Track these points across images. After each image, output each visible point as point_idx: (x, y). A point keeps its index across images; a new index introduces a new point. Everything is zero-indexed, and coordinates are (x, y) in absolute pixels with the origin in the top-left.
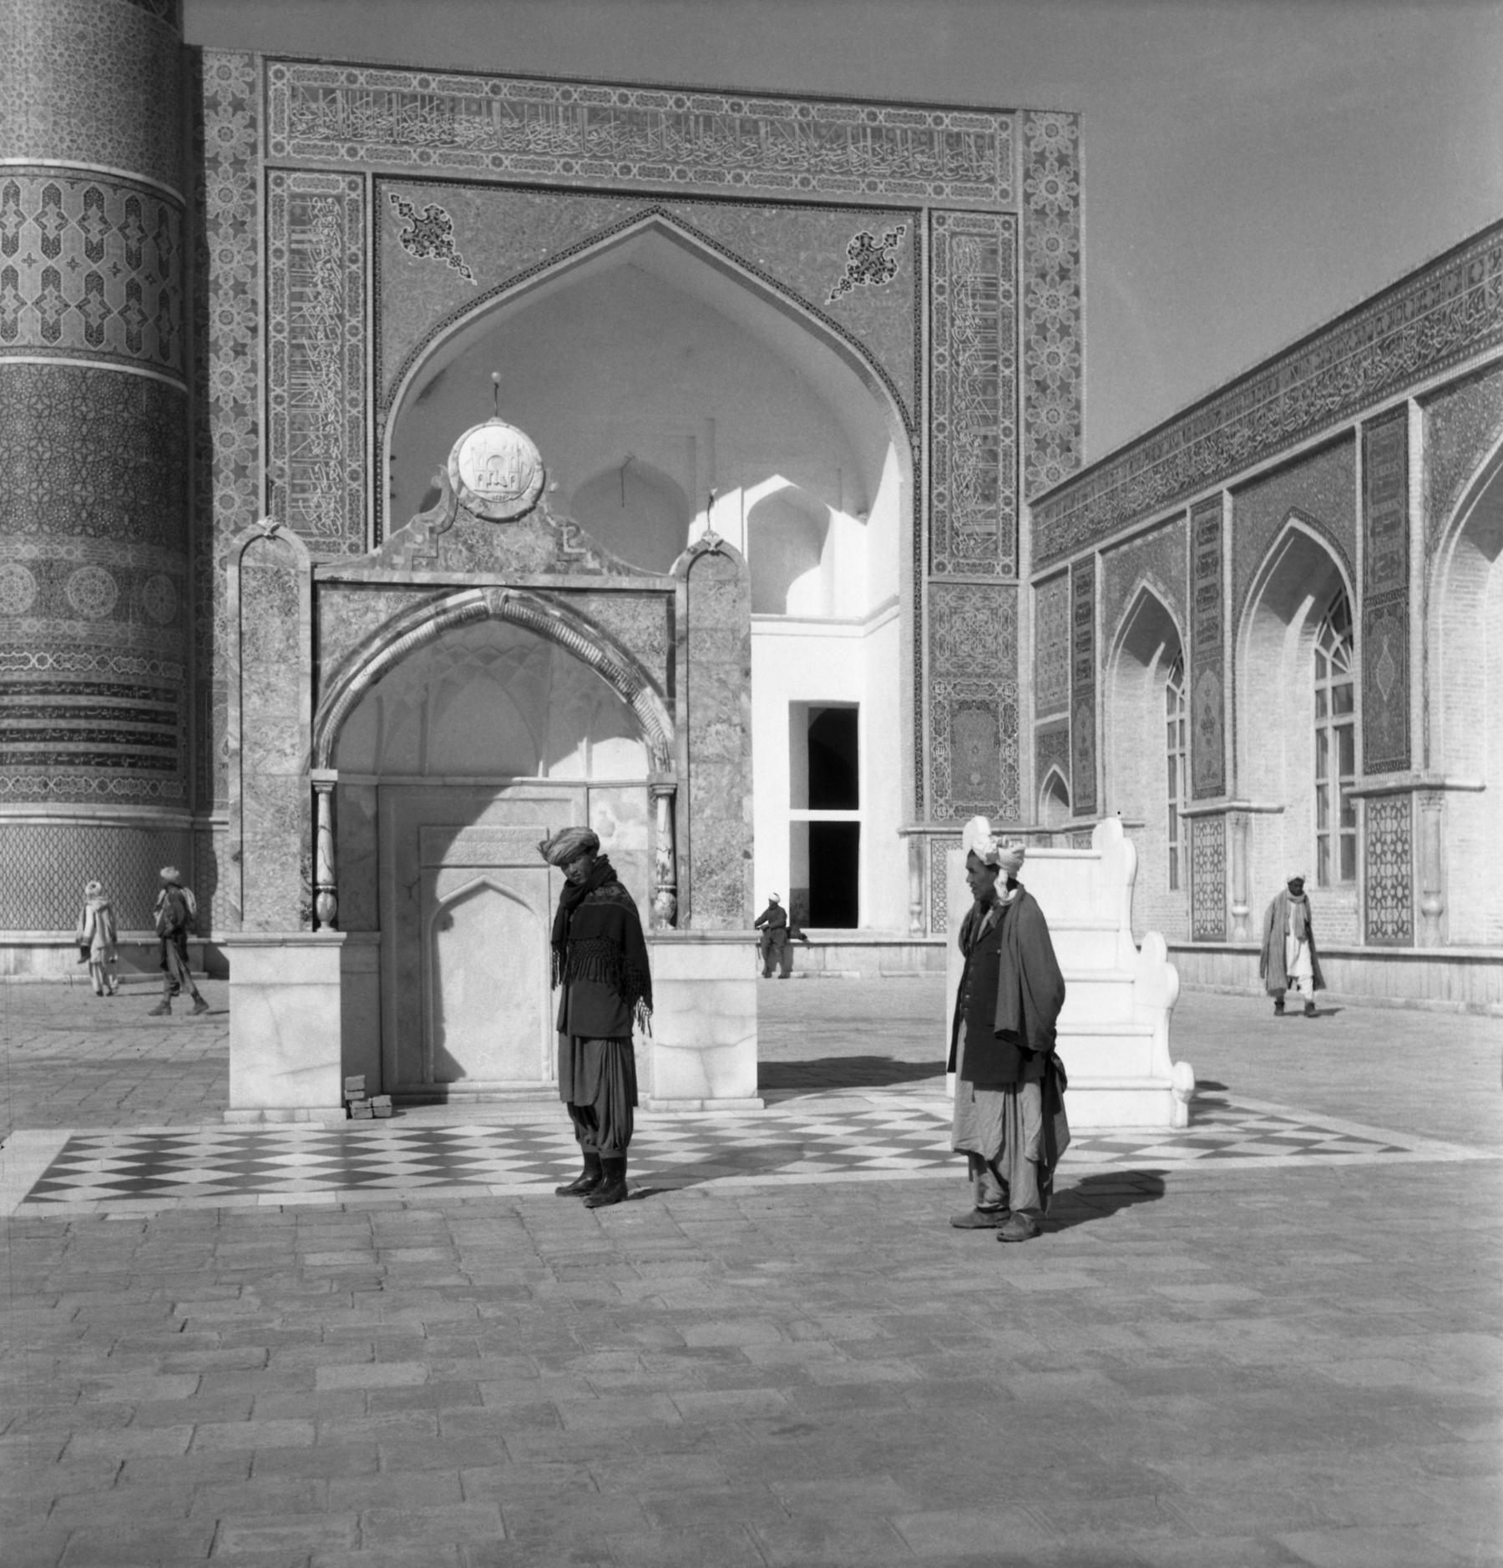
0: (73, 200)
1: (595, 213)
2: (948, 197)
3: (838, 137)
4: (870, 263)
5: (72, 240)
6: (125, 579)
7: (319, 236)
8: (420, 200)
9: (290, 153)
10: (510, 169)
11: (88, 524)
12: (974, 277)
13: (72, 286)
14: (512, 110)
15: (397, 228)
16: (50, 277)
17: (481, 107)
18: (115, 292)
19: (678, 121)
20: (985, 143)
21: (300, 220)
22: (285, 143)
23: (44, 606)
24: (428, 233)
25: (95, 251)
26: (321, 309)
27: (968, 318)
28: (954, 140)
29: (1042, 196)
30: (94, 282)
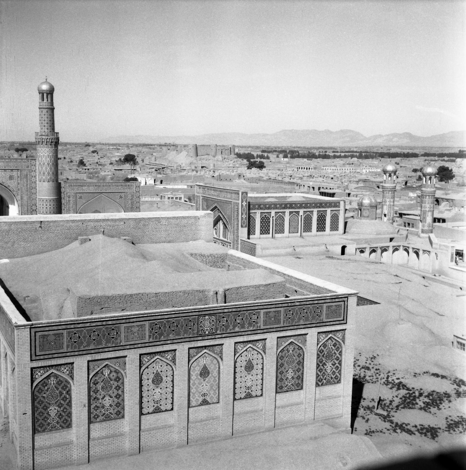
0: (52, 201)
1: (96, 195)
2: (128, 191)
3: (118, 186)
4: (121, 197)
5: (52, 204)
7: (71, 199)
8: (80, 195)
9: (68, 191)
12: (131, 198)
13: (52, 208)
14: (88, 186)
15: (78, 197)
16: (50, 208)
17: (85, 186)
18: (55, 208)
19: (103, 186)
21: (69, 197)
24: (81, 198)
25: (54, 205)
26: (71, 205)
27: (130, 202)
28: (129, 185)
29: (137, 190)
30: (54, 208)
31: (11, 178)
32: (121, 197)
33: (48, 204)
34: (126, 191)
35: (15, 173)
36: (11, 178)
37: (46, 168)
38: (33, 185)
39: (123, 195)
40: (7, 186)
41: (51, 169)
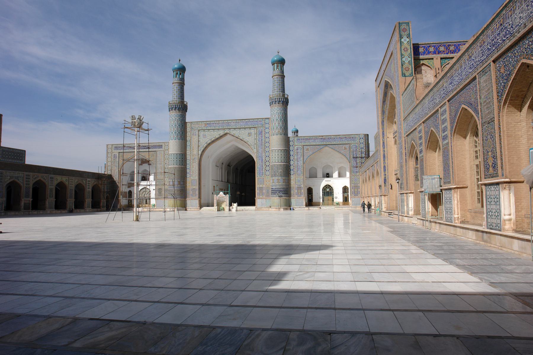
4: (345, 149)
5: (280, 154)
6: (284, 180)
7: (299, 151)
10: (314, 144)
11: (281, 176)
13: (280, 157)
18: (283, 158)
20: (355, 137)
22: (296, 144)
23: (278, 182)
31: (250, 134)
32: (345, 149)
33: (277, 154)
34: (350, 142)
35: (253, 131)
36: (250, 134)
37: (275, 124)
38: (267, 140)
39: (347, 146)
40: (246, 141)
41: (279, 124)
